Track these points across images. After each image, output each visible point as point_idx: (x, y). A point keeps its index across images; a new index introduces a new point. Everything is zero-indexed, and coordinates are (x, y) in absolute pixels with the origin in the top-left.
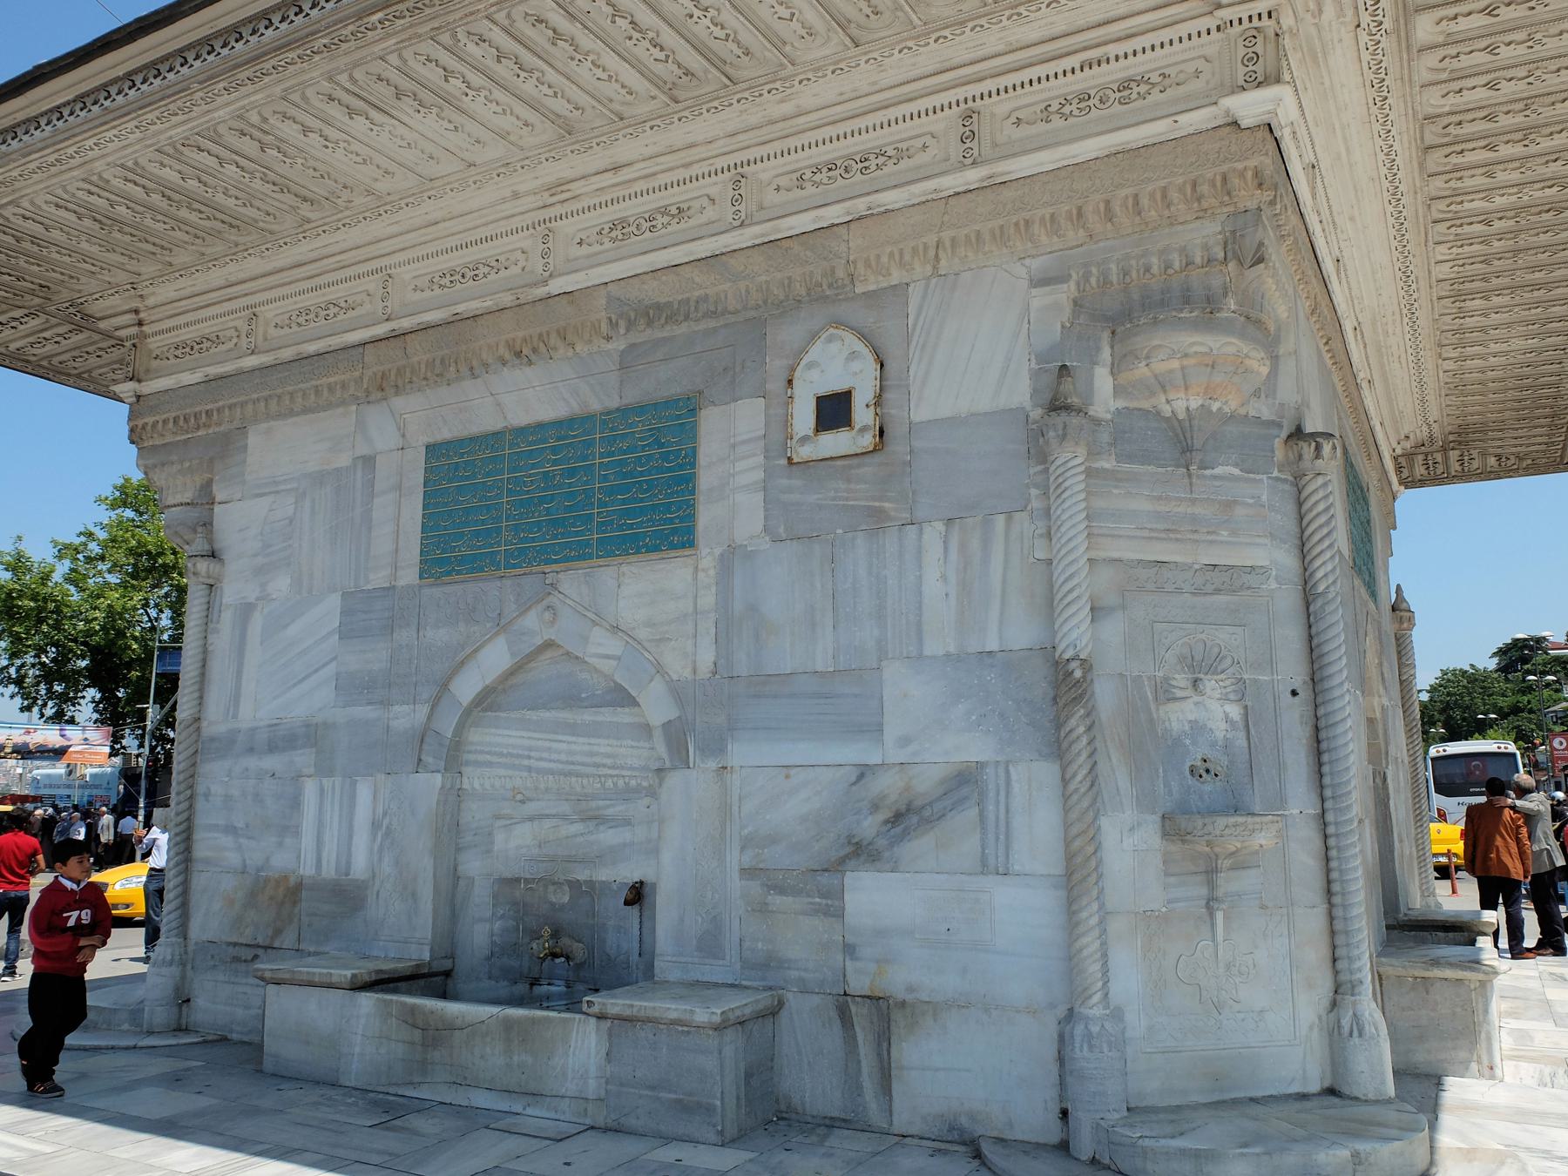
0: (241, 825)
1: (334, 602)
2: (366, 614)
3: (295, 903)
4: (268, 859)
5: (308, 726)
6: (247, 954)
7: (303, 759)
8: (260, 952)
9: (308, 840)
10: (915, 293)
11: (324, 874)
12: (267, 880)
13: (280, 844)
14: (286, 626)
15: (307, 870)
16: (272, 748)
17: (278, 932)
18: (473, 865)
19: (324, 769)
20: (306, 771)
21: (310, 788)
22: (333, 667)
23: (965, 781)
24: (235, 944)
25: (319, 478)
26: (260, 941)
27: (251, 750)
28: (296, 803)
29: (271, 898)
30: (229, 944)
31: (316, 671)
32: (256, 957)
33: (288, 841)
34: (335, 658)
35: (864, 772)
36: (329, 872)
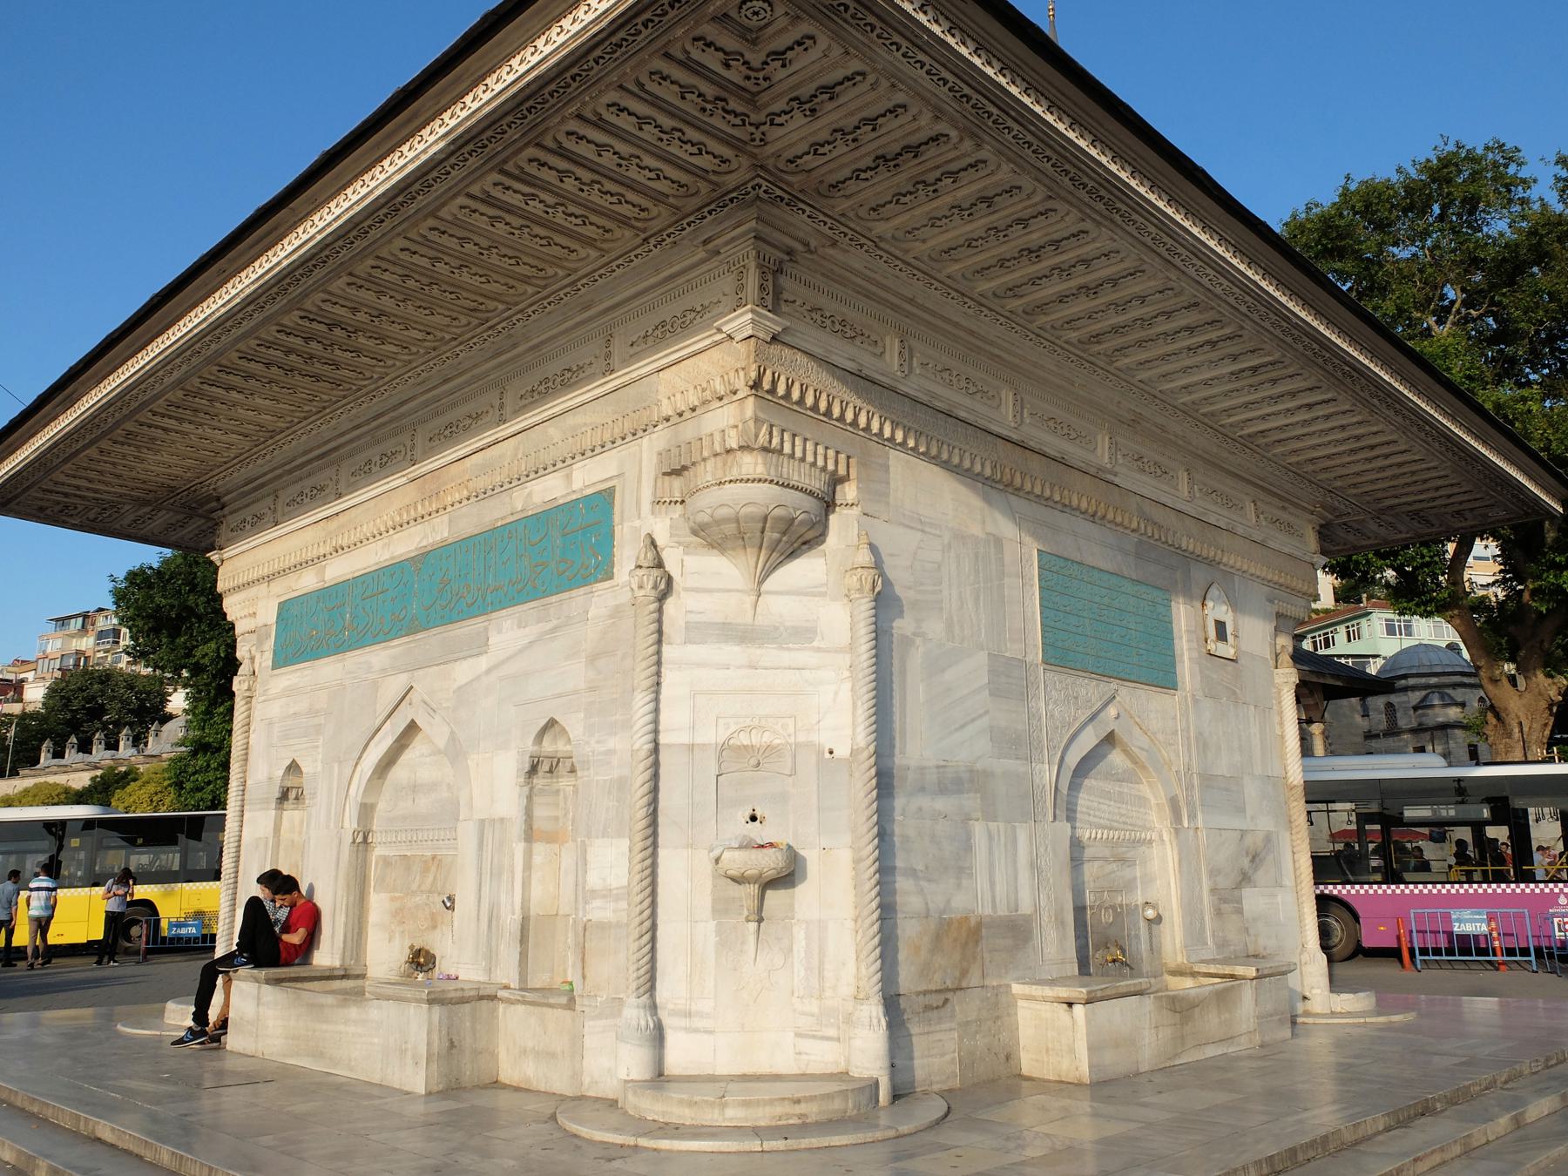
0: (920, 867)
1: (982, 658)
2: (1007, 679)
3: (977, 942)
4: (949, 901)
5: (972, 771)
6: (936, 1000)
7: (970, 802)
8: (949, 995)
9: (982, 882)
10: (1236, 578)
11: (1000, 913)
12: (950, 922)
13: (959, 886)
14: (943, 671)
15: (985, 910)
16: (942, 789)
17: (964, 973)
18: (931, 906)
19: (990, 816)
20: (974, 815)
21: (978, 829)
22: (985, 721)
23: (1268, 838)
24: (925, 993)
25: (960, 537)
26: (949, 984)
27: (922, 789)
28: (968, 847)
29: (955, 940)
30: (918, 994)
31: (973, 720)
32: (946, 1000)
33: (965, 882)
34: (987, 712)
35: (1243, 833)
36: (1002, 911)
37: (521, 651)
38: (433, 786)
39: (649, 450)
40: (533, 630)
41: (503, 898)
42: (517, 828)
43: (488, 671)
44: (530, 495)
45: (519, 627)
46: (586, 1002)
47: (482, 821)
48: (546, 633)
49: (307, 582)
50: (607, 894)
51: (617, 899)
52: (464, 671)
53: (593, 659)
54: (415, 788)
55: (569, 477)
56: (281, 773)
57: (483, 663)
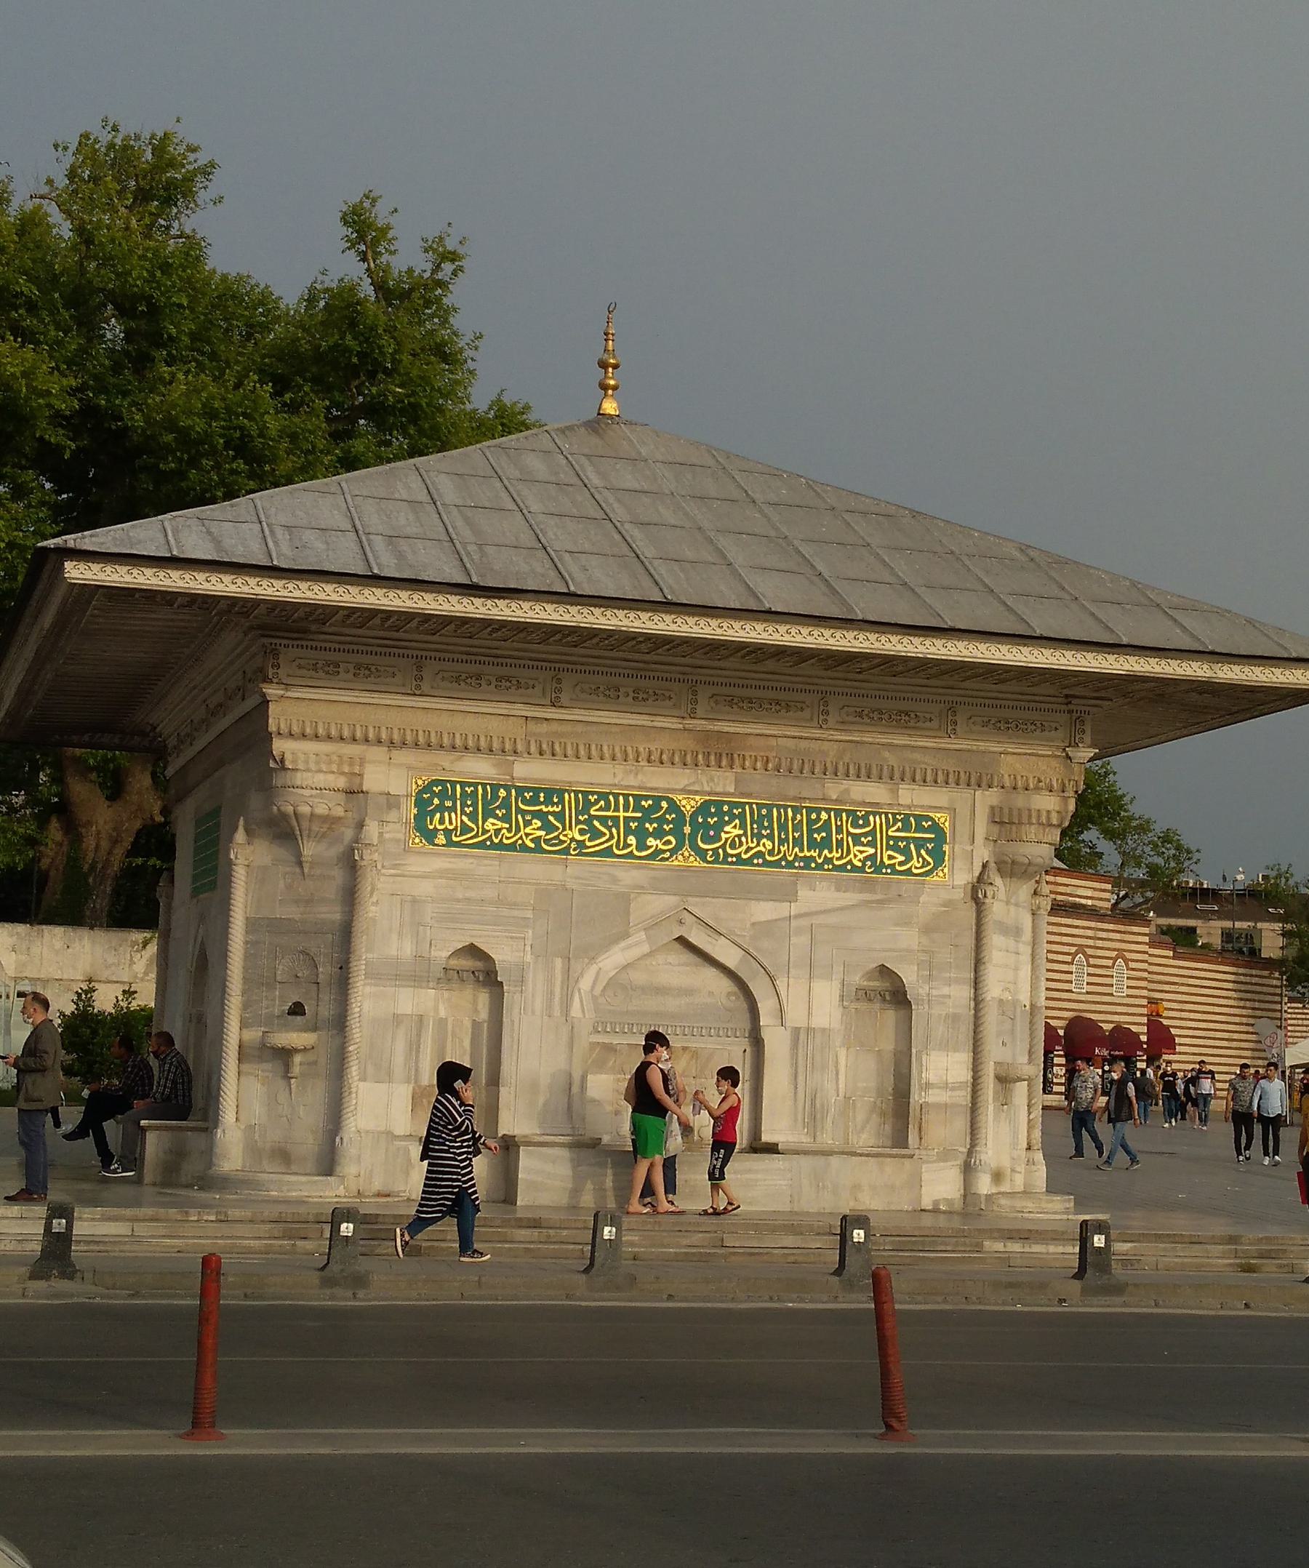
37: (842, 909)
38: (689, 992)
39: (986, 799)
40: (852, 897)
41: (829, 1086)
42: (838, 1040)
43: (798, 916)
44: (847, 791)
45: (838, 890)
46: (924, 1152)
47: (796, 1031)
48: (872, 902)
49: (480, 768)
50: (946, 1086)
51: (953, 1089)
52: (764, 911)
53: (927, 930)
54: (660, 991)
55: (895, 792)
56: (446, 954)
57: (795, 908)
